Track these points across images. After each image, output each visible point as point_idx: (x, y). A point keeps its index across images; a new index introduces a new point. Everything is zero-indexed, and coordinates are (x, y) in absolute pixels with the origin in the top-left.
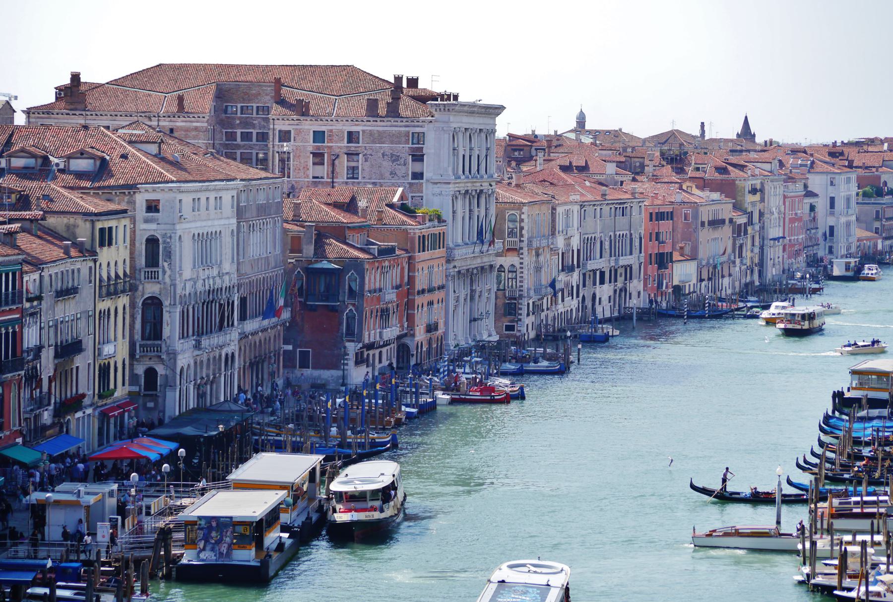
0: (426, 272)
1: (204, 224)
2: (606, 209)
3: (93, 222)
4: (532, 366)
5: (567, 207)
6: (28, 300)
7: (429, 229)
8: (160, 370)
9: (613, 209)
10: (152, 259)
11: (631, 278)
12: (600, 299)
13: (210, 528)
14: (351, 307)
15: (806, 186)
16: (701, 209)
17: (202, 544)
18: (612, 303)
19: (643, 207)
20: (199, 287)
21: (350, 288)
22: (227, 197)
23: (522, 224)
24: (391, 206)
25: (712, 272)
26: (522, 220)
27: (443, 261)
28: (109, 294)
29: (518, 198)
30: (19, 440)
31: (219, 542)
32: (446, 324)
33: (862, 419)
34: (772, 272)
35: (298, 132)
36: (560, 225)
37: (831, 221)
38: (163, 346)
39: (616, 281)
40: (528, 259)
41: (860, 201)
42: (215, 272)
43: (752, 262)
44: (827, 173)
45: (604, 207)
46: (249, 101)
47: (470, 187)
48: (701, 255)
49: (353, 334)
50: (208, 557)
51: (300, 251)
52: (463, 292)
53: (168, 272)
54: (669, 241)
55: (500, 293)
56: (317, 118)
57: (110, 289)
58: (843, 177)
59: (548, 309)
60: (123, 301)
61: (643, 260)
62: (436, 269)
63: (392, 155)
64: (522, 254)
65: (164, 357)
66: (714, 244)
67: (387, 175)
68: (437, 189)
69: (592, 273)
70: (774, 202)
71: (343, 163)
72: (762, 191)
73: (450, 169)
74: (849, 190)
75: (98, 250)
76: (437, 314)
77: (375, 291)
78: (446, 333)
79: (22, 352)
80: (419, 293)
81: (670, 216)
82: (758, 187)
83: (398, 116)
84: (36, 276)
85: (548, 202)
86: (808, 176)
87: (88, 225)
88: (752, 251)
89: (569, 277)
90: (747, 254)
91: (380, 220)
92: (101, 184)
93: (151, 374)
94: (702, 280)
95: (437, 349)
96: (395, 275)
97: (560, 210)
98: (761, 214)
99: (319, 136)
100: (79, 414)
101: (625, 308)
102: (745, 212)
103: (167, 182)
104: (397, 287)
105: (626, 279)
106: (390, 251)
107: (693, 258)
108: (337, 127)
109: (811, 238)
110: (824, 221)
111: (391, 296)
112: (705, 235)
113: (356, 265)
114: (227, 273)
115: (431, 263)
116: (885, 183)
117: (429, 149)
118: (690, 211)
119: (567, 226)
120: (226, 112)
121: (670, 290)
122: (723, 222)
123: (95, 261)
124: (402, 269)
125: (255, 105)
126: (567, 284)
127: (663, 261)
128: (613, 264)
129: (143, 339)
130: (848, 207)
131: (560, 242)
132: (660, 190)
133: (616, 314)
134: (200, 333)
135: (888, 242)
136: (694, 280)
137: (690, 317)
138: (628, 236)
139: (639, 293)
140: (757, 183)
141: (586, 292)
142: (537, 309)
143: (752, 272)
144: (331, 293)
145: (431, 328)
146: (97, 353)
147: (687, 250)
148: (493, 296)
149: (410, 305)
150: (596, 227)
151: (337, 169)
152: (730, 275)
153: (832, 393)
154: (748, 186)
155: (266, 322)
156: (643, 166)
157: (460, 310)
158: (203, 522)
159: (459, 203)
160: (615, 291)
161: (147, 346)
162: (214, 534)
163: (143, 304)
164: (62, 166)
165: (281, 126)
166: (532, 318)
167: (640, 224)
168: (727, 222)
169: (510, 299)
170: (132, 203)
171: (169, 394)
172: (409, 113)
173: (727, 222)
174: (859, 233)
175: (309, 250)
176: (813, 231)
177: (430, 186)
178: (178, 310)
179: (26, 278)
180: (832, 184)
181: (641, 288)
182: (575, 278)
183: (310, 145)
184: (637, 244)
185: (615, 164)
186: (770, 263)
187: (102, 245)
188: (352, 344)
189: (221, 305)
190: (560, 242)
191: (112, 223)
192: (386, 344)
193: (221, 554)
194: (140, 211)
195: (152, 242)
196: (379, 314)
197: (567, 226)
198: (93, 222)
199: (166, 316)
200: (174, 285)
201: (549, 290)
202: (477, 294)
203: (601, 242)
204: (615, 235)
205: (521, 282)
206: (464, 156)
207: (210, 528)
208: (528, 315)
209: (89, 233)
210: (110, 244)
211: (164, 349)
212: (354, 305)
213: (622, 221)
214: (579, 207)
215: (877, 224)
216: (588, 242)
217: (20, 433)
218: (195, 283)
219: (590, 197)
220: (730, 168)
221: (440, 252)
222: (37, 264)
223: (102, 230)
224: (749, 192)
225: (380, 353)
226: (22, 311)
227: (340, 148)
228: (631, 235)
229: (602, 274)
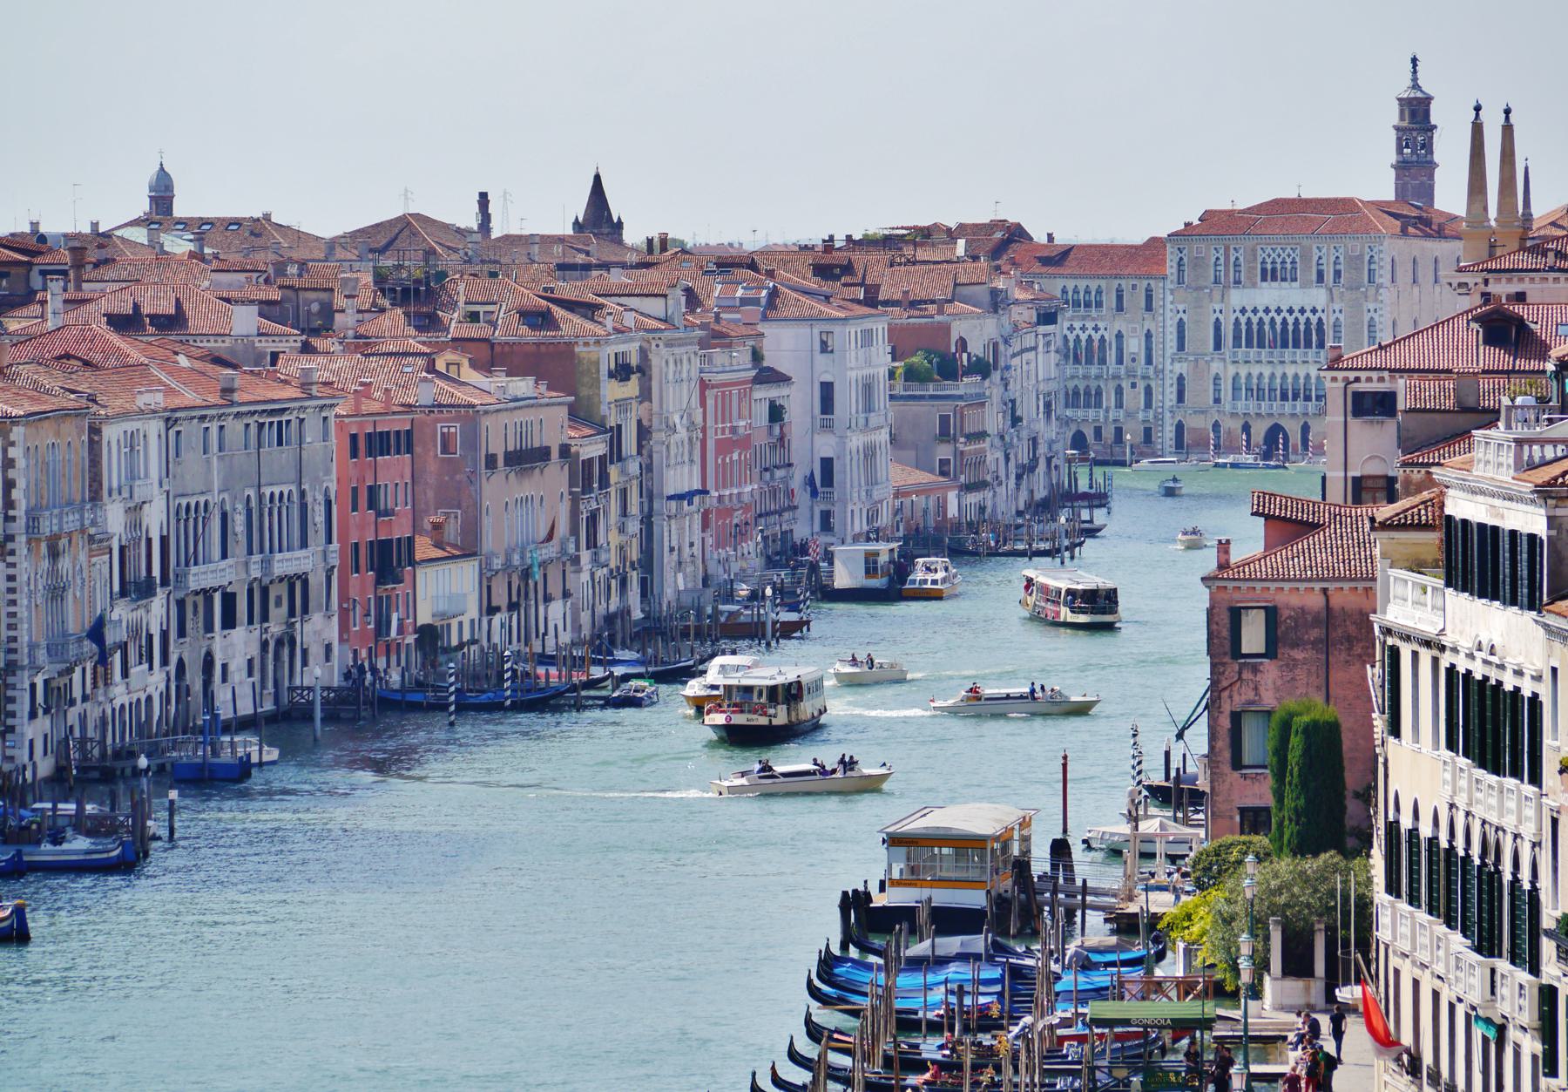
2: (235, 428)
4: (46, 851)
5: (130, 426)
9: (253, 429)
11: (305, 610)
12: (225, 667)
15: (757, 356)
16: (486, 422)
18: (256, 678)
19: (332, 421)
23: (11, 474)
33: (916, 964)
34: (675, 583)
36: (113, 472)
37: (825, 446)
39: (265, 617)
41: (899, 390)
43: (623, 559)
45: (229, 423)
48: (492, 539)
54: (403, 508)
58: (853, 329)
59: (85, 698)
61: (336, 562)
64: (12, 553)
66: (521, 512)
69: (200, 599)
70: (676, 398)
72: (643, 370)
74: (869, 362)
81: (404, 442)
82: (634, 361)
85: (77, 413)
86: (761, 328)
88: (622, 530)
89: (141, 612)
90: (609, 537)
94: (492, 610)
97: (112, 433)
98: (643, 432)
101: (292, 689)
102: (601, 427)
105: (292, 613)
107: (468, 550)
109: (774, 492)
110: (808, 445)
112: (497, 490)
116: (963, 344)
118: (455, 429)
119: (132, 476)
121: (410, 639)
122: (543, 454)
126: (135, 631)
127: (388, 561)
130: (869, 408)
131: (114, 518)
132: (381, 373)
133: (268, 706)
135: (973, 498)
136: (473, 611)
137: (462, 708)
138: (295, 498)
139: (328, 648)
140: (631, 350)
142: (56, 698)
143: (624, 584)
147: (452, 531)
150: (207, 477)
152: (566, 594)
153: (837, 898)
154: (606, 357)
156: (328, 312)
160: (264, 645)
166: (44, 723)
167: (326, 466)
168: (555, 454)
173: (555, 454)
174: (897, 474)
176: (779, 473)
180: (824, 348)
181: (333, 633)
182: (156, 613)
184: (320, 518)
185: (255, 309)
186: (669, 560)
190: (114, 518)
197: (132, 476)
201: (89, 647)
203: (224, 516)
204: (260, 497)
208: (33, 715)
213: (278, 459)
214: (162, 424)
215: (944, 451)
216: (187, 517)
219: (190, 397)
224: (611, 375)
228: (302, 494)
229: (229, 600)
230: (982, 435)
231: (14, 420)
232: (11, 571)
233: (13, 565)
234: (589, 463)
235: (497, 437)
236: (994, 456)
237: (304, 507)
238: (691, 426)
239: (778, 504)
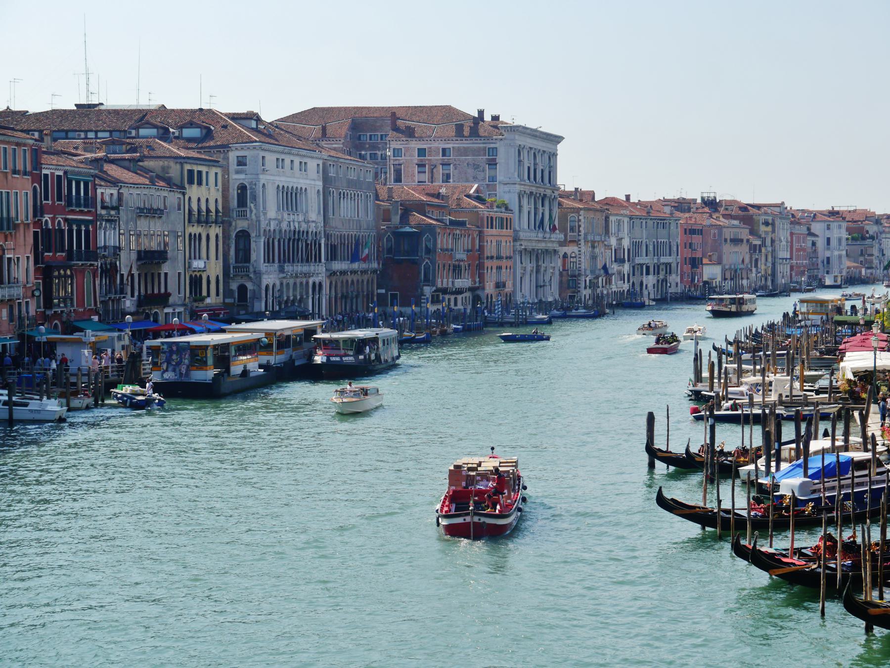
0: (494, 244)
1: (289, 179)
2: (650, 223)
3: (182, 164)
4: (574, 312)
5: (619, 218)
6: (103, 207)
7: (496, 213)
8: (250, 286)
10: (242, 202)
11: (670, 273)
13: (171, 352)
15: (809, 229)
16: (724, 230)
17: (165, 366)
20: (284, 226)
21: (426, 246)
22: (312, 165)
24: (469, 196)
25: (733, 274)
26: (579, 221)
28: (199, 222)
29: (577, 205)
30: (96, 318)
31: (179, 364)
32: (514, 285)
35: (407, 149)
36: (613, 228)
37: (828, 254)
38: (251, 267)
39: (658, 273)
40: (585, 249)
41: (850, 242)
42: (301, 218)
44: (825, 221)
45: (648, 221)
46: (376, 131)
47: (534, 189)
48: (725, 261)
49: (428, 281)
50: (169, 376)
51: (389, 220)
52: (530, 266)
53: (254, 211)
54: (700, 250)
55: (564, 273)
56: (421, 138)
57: (203, 219)
58: (836, 224)
60: (215, 231)
61: (679, 260)
62: (503, 244)
63: (474, 165)
65: (252, 275)
66: (735, 255)
67: (471, 179)
68: (507, 188)
71: (440, 171)
72: (773, 224)
73: (516, 174)
75: (187, 186)
76: (505, 275)
77: (447, 250)
78: (514, 292)
79: (97, 248)
80: (487, 258)
81: (700, 232)
82: (770, 221)
83: (479, 136)
84: (114, 191)
85: (602, 211)
87: (178, 166)
90: (762, 266)
91: (459, 205)
92: (205, 144)
93: (242, 289)
94: (725, 279)
95: (508, 303)
96: (465, 242)
97: (612, 219)
98: (773, 241)
99: (422, 152)
100: (166, 310)
102: (759, 237)
103: (253, 142)
104: (468, 251)
106: (463, 224)
108: (435, 145)
109: (813, 264)
111: (461, 255)
112: (727, 249)
113: (430, 229)
114: (313, 222)
115: (499, 239)
116: (867, 232)
117: (501, 158)
120: (359, 138)
121: (701, 284)
122: (742, 241)
123: (184, 194)
124: (473, 240)
125: (379, 134)
126: (619, 273)
127: (695, 263)
128: (656, 261)
129: (236, 262)
130: (840, 244)
133: (659, 297)
134: (283, 261)
135: (869, 271)
136: (719, 279)
141: (636, 280)
142: (593, 285)
143: (766, 279)
144: (414, 250)
145: (499, 285)
146: (188, 266)
147: (715, 258)
148: (557, 273)
149: (480, 266)
150: (642, 235)
151: (435, 176)
152: (748, 278)
154: (762, 219)
155: (356, 266)
157: (527, 277)
158: (165, 347)
159: (525, 201)
160: (658, 281)
161: (238, 267)
162: (174, 357)
163: (236, 236)
164: (177, 134)
165: (395, 145)
167: (678, 238)
168: (745, 241)
170: (227, 159)
171: (256, 304)
172: (486, 134)
173: (745, 241)
175: (396, 219)
177: (502, 186)
178: (262, 240)
179: (99, 191)
180: (828, 228)
181: (679, 280)
183: (416, 158)
186: (779, 275)
187: (191, 182)
189: (307, 245)
190: (613, 242)
191: (204, 169)
193: (181, 374)
194: (233, 166)
195: (243, 188)
196: (451, 268)
198: (182, 164)
199: (253, 245)
200: (259, 221)
202: (542, 269)
206: (529, 168)
207: (171, 352)
208: (585, 288)
209: (179, 173)
210: (200, 183)
211: (251, 270)
212: (429, 259)
213: (662, 232)
215: (862, 259)
216: (636, 246)
217: (96, 313)
218: (280, 223)
220: (749, 208)
221: (509, 232)
222: (114, 182)
223: (191, 172)
225: (456, 299)
226: (97, 217)
227: (437, 160)
229: (648, 268)
230: (872, 255)
231: (581, 209)
234: (755, 245)
235: (728, 234)
236: (876, 262)
237: (670, 246)
238: (787, 242)
239: (814, 266)
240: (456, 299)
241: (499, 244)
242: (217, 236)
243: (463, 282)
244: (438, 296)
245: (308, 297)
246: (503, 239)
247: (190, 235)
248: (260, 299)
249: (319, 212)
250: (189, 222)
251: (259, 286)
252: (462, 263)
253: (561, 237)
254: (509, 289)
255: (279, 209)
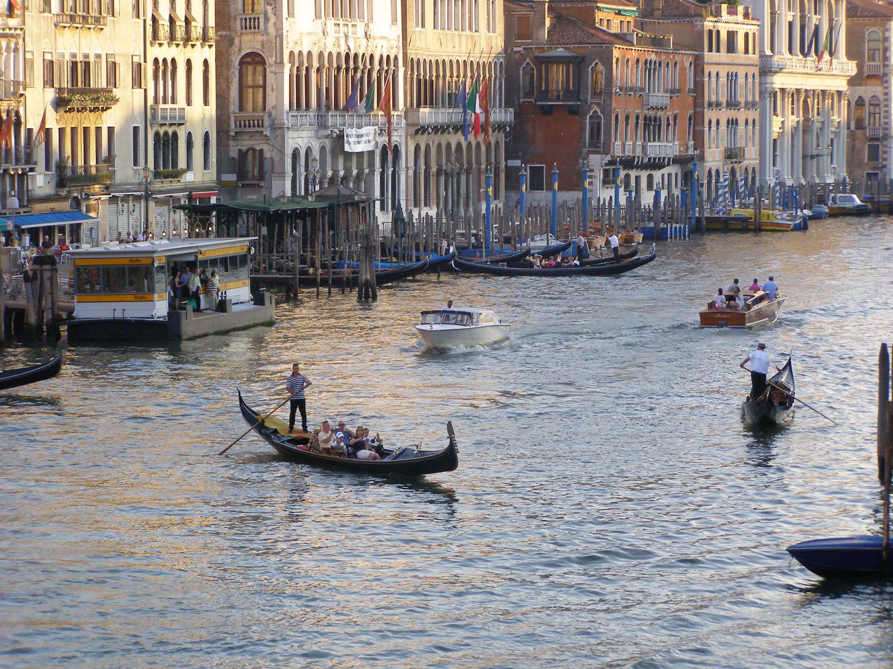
0: (723, 79)
14: (595, 108)
23: (886, 44)
27: (756, 71)
38: (266, 118)
62: (741, 80)
104: (672, 91)
124: (683, 70)
145: (732, 155)
149: (697, 119)
169: (871, 139)
188: (598, 157)
192: (656, 164)
196: (641, 122)
205: (886, 117)
212: (599, 105)
225: (650, 177)
232: (886, 91)
233: (887, 88)
240: (650, 177)
241: (732, 78)
242: (206, 63)
243: (667, 147)
244: (616, 172)
245: (372, 172)
246: (741, 72)
247: (156, 61)
248: (282, 175)
249: (394, 21)
250: (155, 36)
251: (282, 152)
252: (660, 113)
253: (852, 68)
254: (751, 158)
255: (317, 16)
